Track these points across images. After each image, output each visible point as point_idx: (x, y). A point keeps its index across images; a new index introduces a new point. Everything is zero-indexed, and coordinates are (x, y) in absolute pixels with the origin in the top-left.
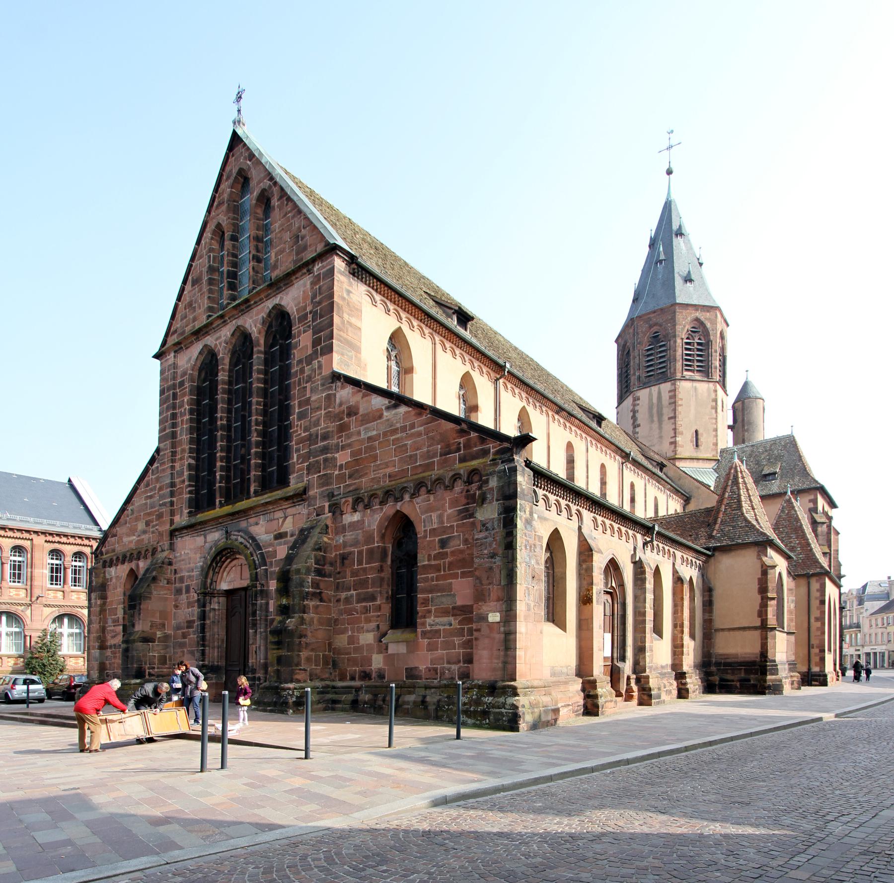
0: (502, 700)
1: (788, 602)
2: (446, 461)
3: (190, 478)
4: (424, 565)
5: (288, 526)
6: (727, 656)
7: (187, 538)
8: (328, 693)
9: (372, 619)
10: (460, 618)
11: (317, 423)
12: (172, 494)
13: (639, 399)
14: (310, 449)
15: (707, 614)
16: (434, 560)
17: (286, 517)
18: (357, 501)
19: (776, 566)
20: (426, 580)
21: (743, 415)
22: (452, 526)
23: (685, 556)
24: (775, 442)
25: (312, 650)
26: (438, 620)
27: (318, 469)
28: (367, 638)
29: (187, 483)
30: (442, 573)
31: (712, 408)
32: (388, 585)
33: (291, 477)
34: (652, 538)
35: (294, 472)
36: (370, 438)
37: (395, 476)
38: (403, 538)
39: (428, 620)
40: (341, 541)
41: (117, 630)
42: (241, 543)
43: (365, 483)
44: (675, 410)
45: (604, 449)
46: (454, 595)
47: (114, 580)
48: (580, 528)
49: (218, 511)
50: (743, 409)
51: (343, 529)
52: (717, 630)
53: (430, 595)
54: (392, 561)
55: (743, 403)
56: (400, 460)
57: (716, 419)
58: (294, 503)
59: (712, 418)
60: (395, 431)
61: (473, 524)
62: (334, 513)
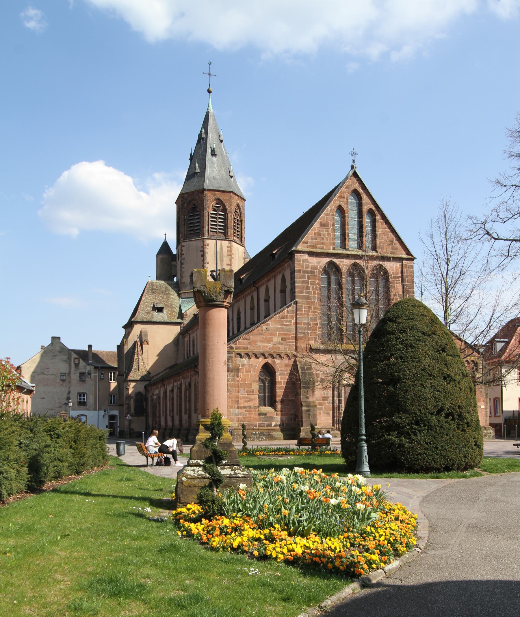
0: (489, 431)
41: (251, 397)
44: (231, 260)
49: (345, 347)
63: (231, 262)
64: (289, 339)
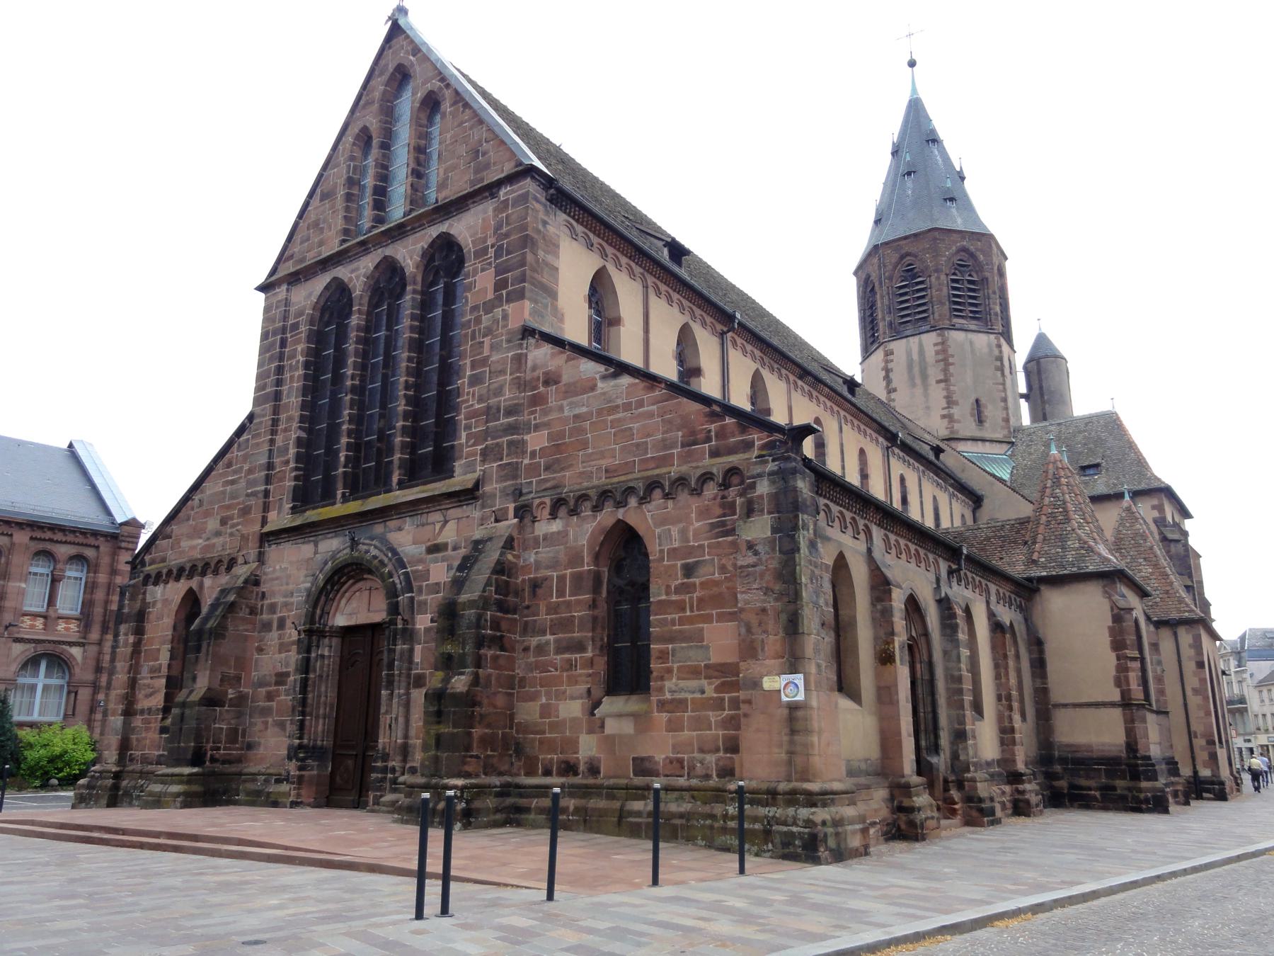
1: (1152, 665)
2: (690, 454)
3: (298, 458)
4: (660, 602)
5: (449, 535)
6: (1074, 748)
7: (288, 545)
8: (508, 795)
9: (579, 679)
10: (717, 682)
11: (499, 392)
12: (268, 480)
13: (892, 353)
14: (488, 428)
15: (1038, 680)
16: (676, 593)
17: (446, 522)
18: (558, 504)
19: (1132, 609)
20: (663, 623)
21: (1040, 380)
22: (701, 547)
23: (1001, 591)
24: (1089, 420)
25: (489, 726)
26: (682, 684)
27: (498, 456)
28: (572, 709)
29: (292, 465)
30: (688, 613)
31: (997, 369)
32: (603, 628)
33: (456, 464)
34: (959, 564)
35: (461, 458)
36: (576, 417)
37: (615, 471)
38: (624, 559)
39: (668, 684)
40: (532, 560)
42: (375, 557)
43: (570, 480)
45: (862, 427)
46: (707, 648)
47: (159, 605)
48: (869, 551)
50: (1039, 372)
51: (536, 542)
52: (1057, 706)
53: (670, 646)
54: (608, 592)
55: (1038, 363)
56: (623, 449)
57: (1004, 384)
58: (460, 501)
59: (997, 384)
60: (615, 409)
61: (734, 544)
62: (521, 519)
63: (945, 375)
64: (232, 518)
